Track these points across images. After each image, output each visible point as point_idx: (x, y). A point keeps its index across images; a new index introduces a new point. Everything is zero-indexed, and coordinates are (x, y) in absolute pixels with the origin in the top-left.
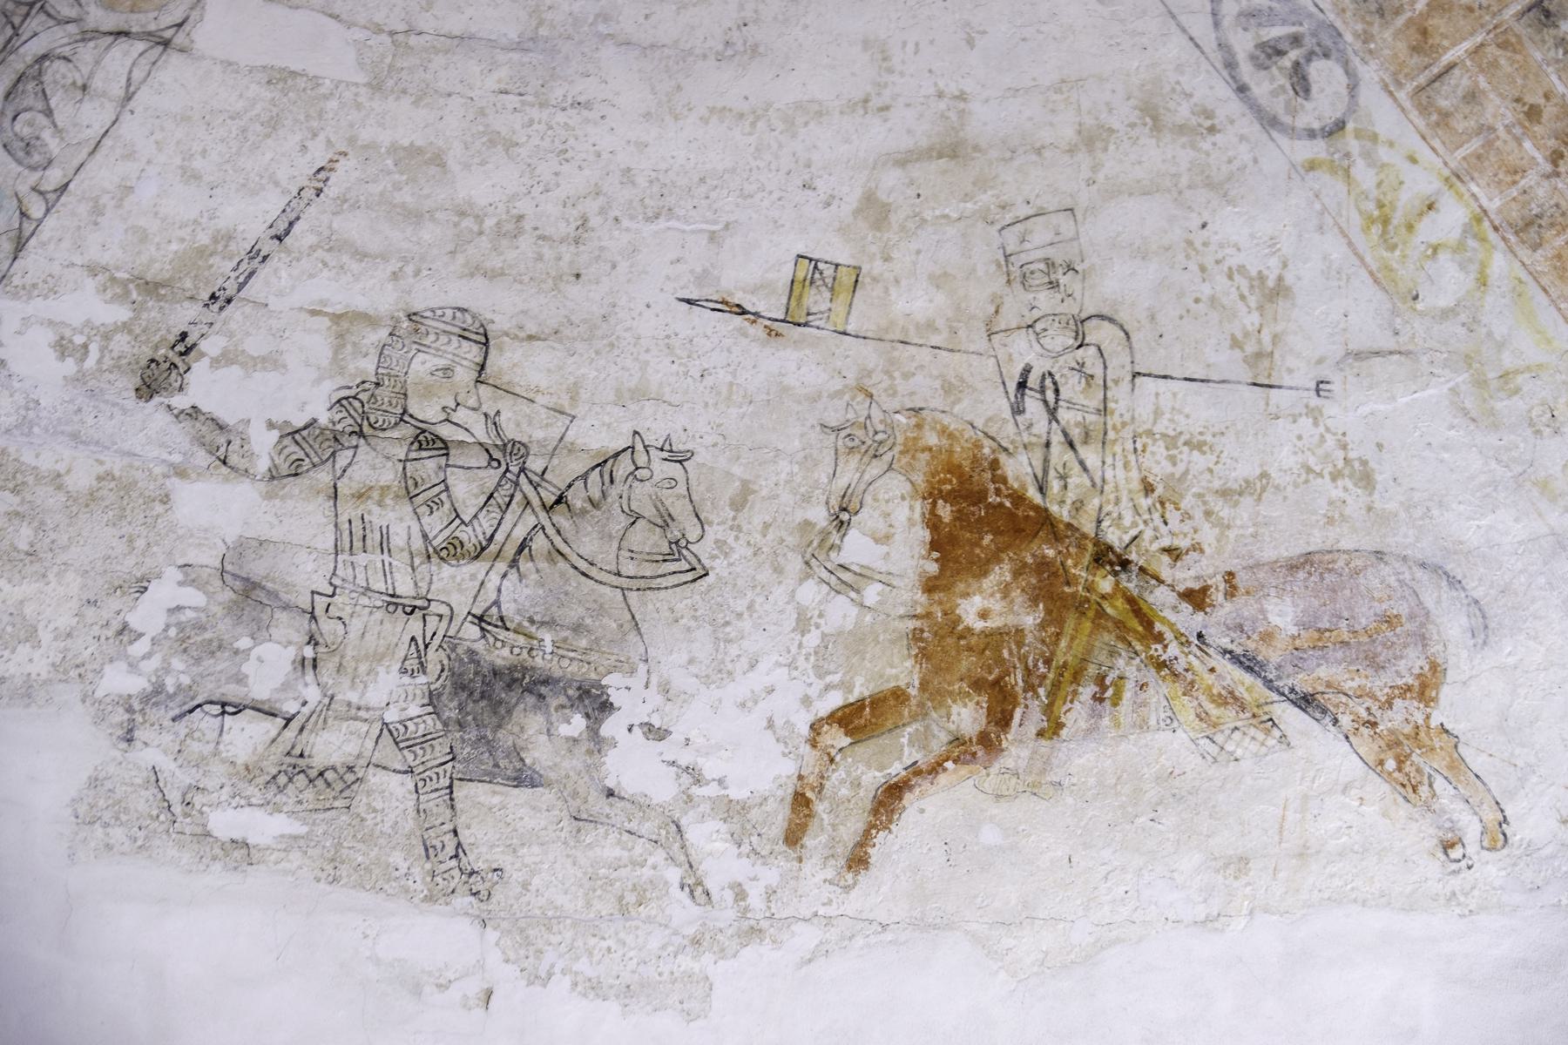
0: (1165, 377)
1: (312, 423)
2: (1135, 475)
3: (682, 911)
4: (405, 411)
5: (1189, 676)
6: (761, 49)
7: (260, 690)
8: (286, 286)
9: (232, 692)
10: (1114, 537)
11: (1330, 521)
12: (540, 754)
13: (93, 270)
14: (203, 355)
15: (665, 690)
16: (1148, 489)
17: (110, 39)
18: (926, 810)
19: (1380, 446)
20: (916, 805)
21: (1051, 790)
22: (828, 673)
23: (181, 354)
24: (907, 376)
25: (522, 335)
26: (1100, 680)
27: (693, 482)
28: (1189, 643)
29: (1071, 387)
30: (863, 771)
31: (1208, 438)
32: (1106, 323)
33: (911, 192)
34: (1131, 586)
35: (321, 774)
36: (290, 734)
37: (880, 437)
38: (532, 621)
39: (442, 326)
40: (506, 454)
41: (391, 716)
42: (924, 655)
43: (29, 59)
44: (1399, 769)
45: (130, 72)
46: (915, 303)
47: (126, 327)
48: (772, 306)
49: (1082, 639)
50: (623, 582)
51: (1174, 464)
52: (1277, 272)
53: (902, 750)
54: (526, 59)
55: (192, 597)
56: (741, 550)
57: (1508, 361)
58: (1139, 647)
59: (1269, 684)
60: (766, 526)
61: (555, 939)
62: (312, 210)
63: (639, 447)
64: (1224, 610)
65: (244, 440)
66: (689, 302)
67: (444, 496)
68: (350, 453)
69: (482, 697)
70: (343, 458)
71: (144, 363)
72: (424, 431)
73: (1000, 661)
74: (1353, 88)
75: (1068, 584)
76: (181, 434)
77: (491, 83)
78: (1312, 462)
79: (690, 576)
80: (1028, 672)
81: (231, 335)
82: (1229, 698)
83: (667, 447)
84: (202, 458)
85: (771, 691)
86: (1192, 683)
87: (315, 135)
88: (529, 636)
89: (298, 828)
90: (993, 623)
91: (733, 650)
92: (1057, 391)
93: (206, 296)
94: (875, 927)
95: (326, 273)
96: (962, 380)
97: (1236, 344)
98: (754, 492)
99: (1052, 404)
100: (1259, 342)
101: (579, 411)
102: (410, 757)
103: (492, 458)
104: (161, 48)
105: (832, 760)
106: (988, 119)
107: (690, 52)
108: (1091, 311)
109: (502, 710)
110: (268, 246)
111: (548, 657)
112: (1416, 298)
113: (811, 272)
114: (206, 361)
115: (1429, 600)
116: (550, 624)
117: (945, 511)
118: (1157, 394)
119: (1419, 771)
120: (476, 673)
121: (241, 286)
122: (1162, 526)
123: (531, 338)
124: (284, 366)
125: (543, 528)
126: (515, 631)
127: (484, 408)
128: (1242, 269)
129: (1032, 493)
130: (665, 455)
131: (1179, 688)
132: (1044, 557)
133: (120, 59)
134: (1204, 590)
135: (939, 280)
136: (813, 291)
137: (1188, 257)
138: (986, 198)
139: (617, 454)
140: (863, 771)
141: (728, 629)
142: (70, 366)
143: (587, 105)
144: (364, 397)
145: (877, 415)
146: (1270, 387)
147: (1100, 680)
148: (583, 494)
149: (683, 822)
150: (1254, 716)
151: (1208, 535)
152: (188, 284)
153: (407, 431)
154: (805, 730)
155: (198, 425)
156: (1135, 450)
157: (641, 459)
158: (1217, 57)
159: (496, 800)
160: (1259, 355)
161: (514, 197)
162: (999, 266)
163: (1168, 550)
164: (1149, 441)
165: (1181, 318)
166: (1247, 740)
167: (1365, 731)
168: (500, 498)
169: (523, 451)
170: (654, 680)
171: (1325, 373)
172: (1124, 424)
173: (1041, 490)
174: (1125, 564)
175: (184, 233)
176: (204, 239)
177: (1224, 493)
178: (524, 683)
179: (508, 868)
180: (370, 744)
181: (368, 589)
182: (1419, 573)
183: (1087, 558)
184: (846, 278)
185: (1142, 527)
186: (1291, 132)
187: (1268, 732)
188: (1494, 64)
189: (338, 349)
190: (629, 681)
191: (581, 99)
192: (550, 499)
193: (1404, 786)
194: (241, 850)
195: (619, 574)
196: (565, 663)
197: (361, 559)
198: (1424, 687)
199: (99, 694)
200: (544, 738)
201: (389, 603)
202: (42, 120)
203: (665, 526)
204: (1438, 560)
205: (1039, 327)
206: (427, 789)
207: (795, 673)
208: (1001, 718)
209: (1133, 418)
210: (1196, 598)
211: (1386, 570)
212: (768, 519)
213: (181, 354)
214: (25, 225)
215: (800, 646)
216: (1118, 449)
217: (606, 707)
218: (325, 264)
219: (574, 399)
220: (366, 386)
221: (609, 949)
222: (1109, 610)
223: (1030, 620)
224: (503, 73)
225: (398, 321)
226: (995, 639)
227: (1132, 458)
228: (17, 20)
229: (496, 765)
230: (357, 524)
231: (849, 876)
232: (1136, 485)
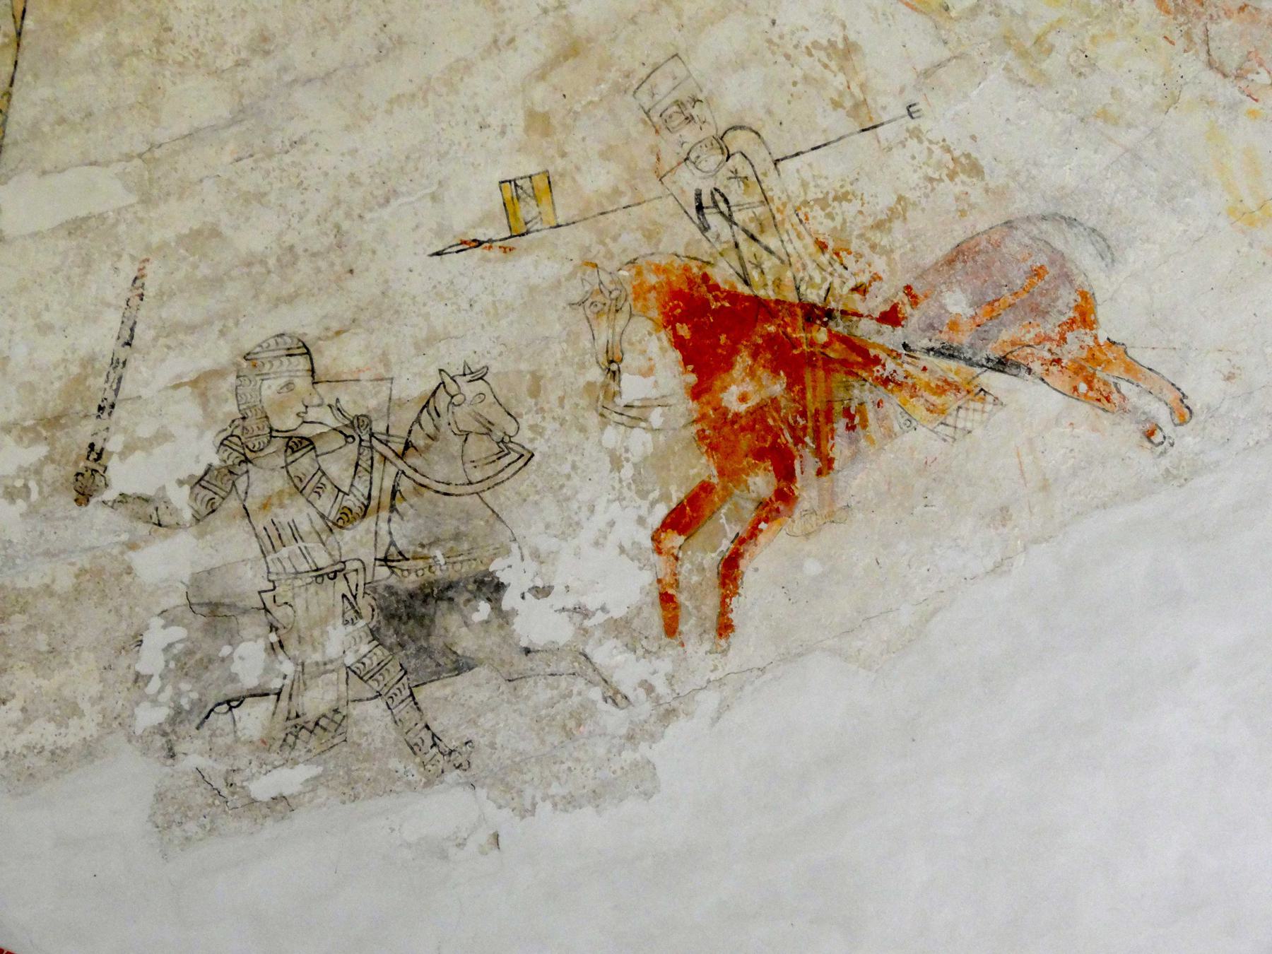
0: (797, 154)
1: (209, 469)
2: (809, 241)
3: (613, 719)
4: (271, 429)
5: (910, 381)
6: (405, 39)
7: (250, 681)
8: (149, 376)
9: (230, 691)
11: (963, 213)
12: (466, 643)
14: (111, 453)
15: (536, 555)
16: (823, 247)
18: (759, 568)
19: (973, 138)
20: (750, 568)
21: (843, 514)
22: (648, 493)
23: (96, 460)
24: (615, 239)
25: (330, 334)
26: (847, 413)
27: (496, 390)
28: (899, 355)
29: (735, 193)
30: (700, 558)
31: (848, 188)
33: (559, 96)
34: (840, 329)
35: (317, 724)
36: (284, 703)
37: (613, 296)
38: (422, 546)
39: (271, 354)
40: (356, 428)
41: (350, 659)
42: (713, 448)
44: (1091, 388)
46: (597, 179)
47: (49, 459)
48: (497, 230)
49: (822, 386)
51: (833, 219)
52: (841, 35)
53: (724, 527)
54: (244, 129)
55: (178, 633)
56: (550, 426)
57: (1036, 28)
58: (865, 375)
59: (969, 361)
60: (561, 400)
61: (528, 777)
62: (143, 312)
63: (447, 380)
64: (914, 317)
65: (167, 503)
66: (438, 254)
67: (324, 480)
68: (245, 478)
69: (409, 618)
70: (241, 484)
71: (72, 479)
72: (290, 438)
73: (768, 429)
75: (795, 348)
76: (118, 519)
77: (227, 158)
78: (930, 172)
79: (521, 462)
80: (792, 429)
81: (125, 430)
83: (467, 371)
84: (143, 529)
85: (612, 524)
86: (914, 386)
87: (119, 256)
88: (425, 558)
89: (315, 770)
90: (751, 403)
91: (574, 505)
92: (726, 201)
93: (95, 410)
94: (756, 672)
95: (172, 354)
96: (654, 223)
97: (836, 105)
98: (542, 377)
99: (727, 213)
100: (852, 95)
101: (395, 371)
102: (375, 684)
103: (347, 437)
105: (677, 559)
107: (356, 66)
108: (723, 126)
109: (427, 622)
110: (123, 353)
111: (444, 568)
112: (947, 9)
113: (514, 191)
114: (115, 458)
115: (1058, 244)
116: (436, 542)
117: (684, 331)
118: (798, 171)
119: (1106, 383)
120: (398, 602)
121: (117, 391)
122: (844, 272)
123: (338, 333)
124: (173, 436)
126: (414, 558)
127: (327, 402)
128: (816, 44)
129: (742, 289)
130: (469, 377)
131: (905, 393)
132: (769, 334)
134: (894, 308)
136: (522, 204)
137: (773, 53)
138: (613, 75)
139: (434, 393)
141: (565, 490)
142: (21, 505)
144: (238, 432)
145: (605, 278)
146: (875, 127)
147: (847, 413)
148: (422, 434)
149: (588, 651)
150: (968, 392)
151: (880, 265)
153: (279, 443)
154: (649, 544)
155: (129, 506)
156: (801, 221)
157: (452, 388)
159: (448, 691)
160: (856, 106)
161: (280, 234)
162: (645, 123)
163: (856, 289)
164: (808, 209)
165: (789, 102)
166: (970, 413)
167: (1055, 369)
168: (365, 464)
169: (366, 421)
170: (526, 552)
171: (910, 97)
173: (746, 282)
174: (829, 314)
175: (60, 371)
176: (75, 369)
177: (879, 226)
178: (435, 594)
179: (475, 738)
180: (343, 687)
181: (297, 573)
182: (1045, 226)
183: (800, 322)
185: (830, 279)
187: (983, 400)
189: (205, 405)
190: (508, 561)
191: (295, 139)
193: (1099, 400)
194: (282, 804)
195: (470, 483)
196: (458, 566)
197: (284, 552)
198: (1083, 315)
199: (139, 732)
200: (464, 629)
201: (316, 577)
203: (489, 433)
204: (1052, 209)
205: (693, 156)
206: (396, 702)
207: (624, 503)
208: (785, 472)
209: (788, 196)
210: (891, 317)
211: (1018, 234)
212: (561, 393)
215: (621, 481)
216: (788, 226)
217: (499, 587)
218: (169, 347)
219: (387, 365)
220: (236, 423)
221: (569, 769)
222: (832, 355)
223: (777, 387)
224: (231, 146)
226: (758, 414)
227: (801, 228)
229: (438, 665)
231: (723, 642)
232: (813, 248)
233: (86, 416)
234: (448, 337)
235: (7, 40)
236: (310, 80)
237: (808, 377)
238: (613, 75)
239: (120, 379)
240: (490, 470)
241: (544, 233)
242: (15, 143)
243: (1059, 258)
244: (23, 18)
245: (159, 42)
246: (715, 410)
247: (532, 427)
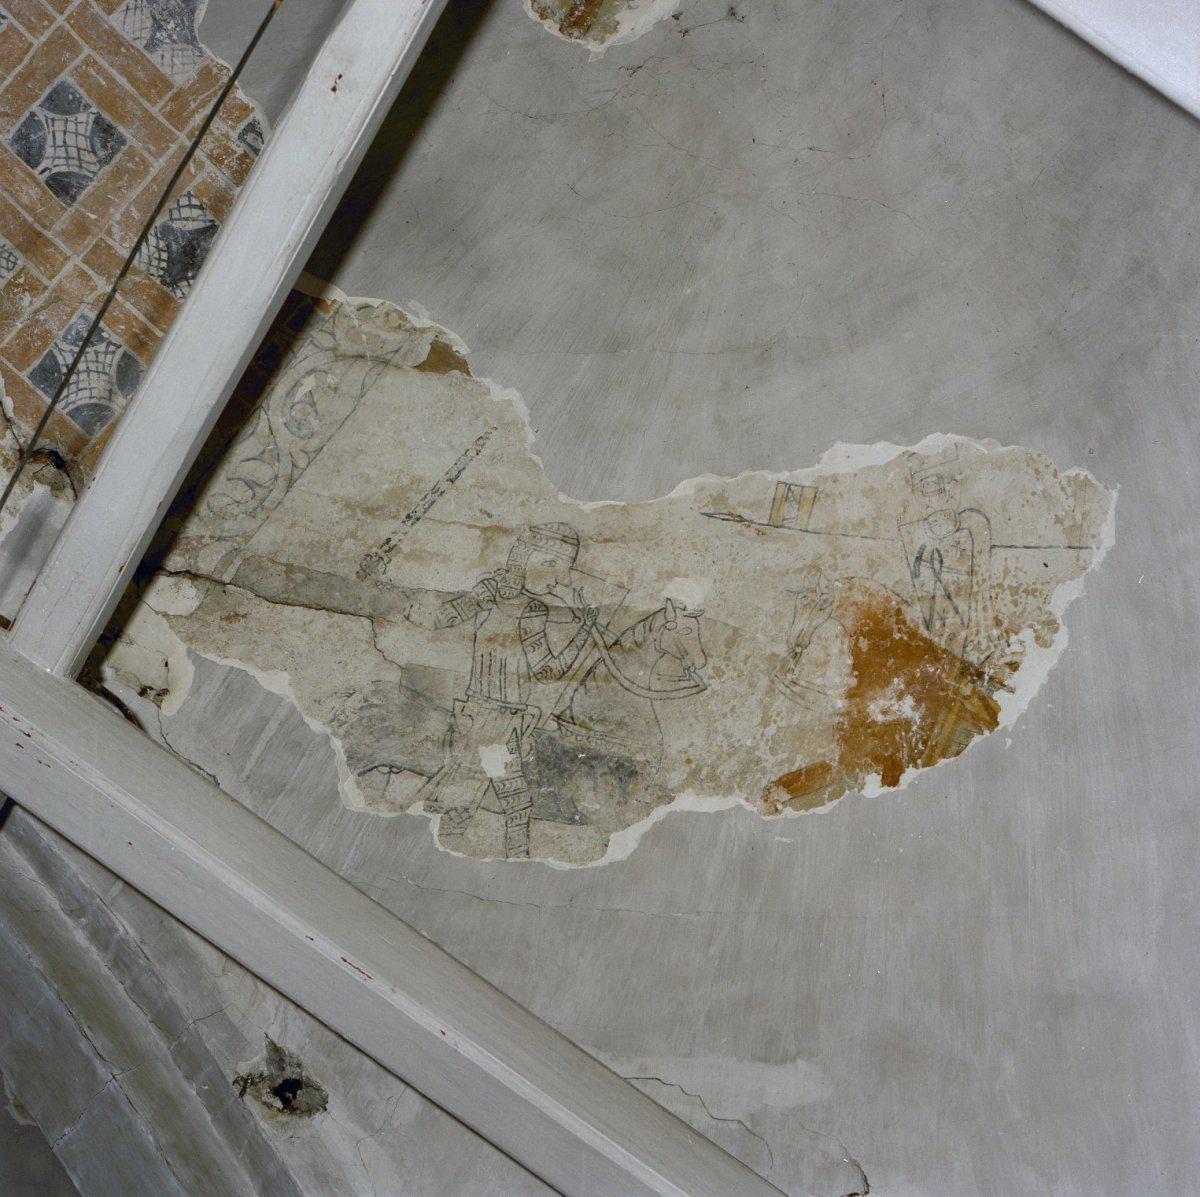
0: (1011, 547)
2: (990, 614)
4: (523, 587)
10: (974, 657)
16: (998, 623)
23: (386, 552)
24: (844, 557)
25: (600, 539)
31: (1039, 586)
32: (974, 514)
36: (430, 787)
37: (824, 597)
38: (591, 719)
40: (585, 617)
42: (845, 740)
45: (364, 380)
48: (761, 517)
50: (654, 695)
51: (1016, 606)
60: (747, 658)
63: (670, 608)
66: (710, 516)
67: (543, 641)
69: (555, 767)
72: (534, 600)
79: (694, 690)
80: (911, 749)
87: (478, 417)
88: (589, 729)
90: (890, 718)
93: (403, 516)
97: (1058, 520)
100: (1073, 519)
101: (635, 586)
103: (575, 616)
108: (965, 505)
116: (603, 721)
117: (864, 644)
118: (1006, 559)
120: (553, 752)
125: (604, 660)
127: (574, 585)
132: (927, 672)
133: (359, 371)
136: (787, 504)
137: (1028, 465)
139: (656, 613)
144: (498, 578)
145: (823, 583)
146: (1080, 548)
152: (393, 510)
153: (525, 600)
156: (991, 597)
157: (670, 615)
159: (556, 833)
162: (907, 481)
165: (1023, 506)
168: (578, 642)
172: (984, 580)
173: (928, 628)
175: (391, 478)
176: (405, 481)
180: (480, 794)
184: (809, 494)
185: (993, 649)
192: (610, 641)
195: (649, 689)
201: (502, 707)
202: (310, 409)
203: (682, 658)
205: (931, 519)
206: (513, 824)
209: (990, 577)
212: (748, 653)
213: (386, 552)
214: (295, 472)
215: (763, 735)
216: (979, 597)
222: (969, 707)
227: (988, 603)
229: (559, 811)
230: (486, 659)
232: (990, 622)
233: (395, 517)
237: (941, 717)
239: (433, 503)
241: (793, 532)
246: (859, 712)
247: (714, 668)
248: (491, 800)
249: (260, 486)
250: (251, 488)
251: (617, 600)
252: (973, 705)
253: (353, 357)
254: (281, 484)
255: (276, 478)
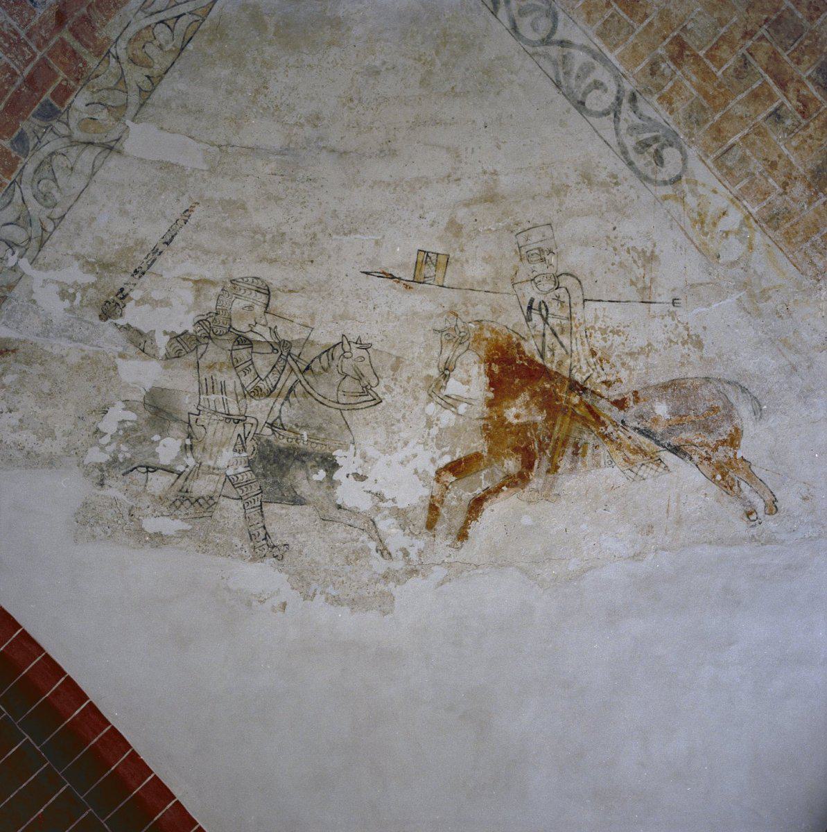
0: (599, 301)
1: (185, 332)
2: (587, 348)
3: (379, 564)
4: (231, 326)
5: (619, 441)
8: (174, 266)
9: (151, 461)
10: (578, 377)
11: (683, 364)
12: (304, 489)
13: (77, 257)
14: (132, 299)
15: (364, 457)
16: (594, 354)
17: (81, 147)
18: (494, 510)
19: (705, 328)
20: (489, 508)
21: (555, 498)
22: (443, 446)
23: (121, 299)
24: (474, 305)
25: (286, 290)
26: (576, 445)
27: (373, 359)
28: (618, 425)
29: (554, 308)
30: (460, 494)
31: (622, 328)
32: (569, 277)
34: (588, 400)
35: (197, 500)
36: (181, 481)
37: (462, 334)
39: (246, 286)
40: (281, 347)
41: (230, 472)
42: (490, 436)
43: (46, 154)
44: (723, 479)
45: (94, 162)
46: (476, 271)
47: (94, 285)
49: (566, 426)
51: (606, 342)
52: (651, 249)
53: (482, 481)
55: (131, 416)
56: (398, 390)
57: (764, 285)
58: (593, 429)
59: (657, 442)
60: (409, 378)
61: (317, 578)
63: (345, 342)
64: (633, 409)
65: (153, 340)
66: (367, 273)
67: (251, 367)
68: (205, 346)
70: (201, 349)
71: (103, 303)
72: (240, 336)
74: (684, 160)
75: (557, 400)
76: (120, 337)
77: (267, 170)
78: (672, 337)
79: (373, 403)
80: (540, 443)
81: (145, 290)
82: (639, 450)
83: (359, 342)
84: (132, 350)
85: (415, 456)
86: (620, 444)
89: (186, 526)
90: (520, 421)
91: (396, 437)
92: (547, 310)
93: (132, 271)
94: (473, 566)
96: (500, 306)
97: (632, 283)
99: (545, 316)
100: (644, 282)
102: (240, 492)
103: (274, 349)
104: (108, 151)
105: (447, 488)
106: (505, 183)
108: (561, 271)
109: (284, 468)
111: (306, 443)
112: (719, 257)
113: (425, 257)
114: (133, 302)
115: (733, 399)
116: (306, 427)
117: (496, 368)
118: (596, 309)
119: (733, 479)
120: (270, 451)
121: (149, 266)
122: (601, 371)
123: (290, 291)
124: (171, 305)
125: (300, 382)
126: (289, 431)
127: (269, 325)
128: (634, 248)
129: (538, 359)
130: (358, 346)
131: (614, 447)
132: (545, 388)
133: (88, 155)
134: (624, 400)
135: (487, 260)
136: (427, 267)
137: (608, 244)
138: (508, 220)
139: (335, 346)
140: (460, 494)
141: (393, 427)
142: (67, 303)
143: (315, 180)
145: (459, 323)
146: (650, 303)
147: (576, 445)
148: (319, 365)
149: (376, 520)
150: (651, 458)
151: (624, 374)
152: (124, 265)
153: (231, 336)
154: (433, 474)
155: (130, 333)
156: (586, 336)
157: (347, 348)
158: (618, 150)
159: (284, 511)
160: (644, 288)
162: (516, 252)
163: (605, 382)
164: (593, 331)
166: (649, 470)
167: (706, 462)
168: (279, 367)
169: (289, 345)
170: (358, 452)
171: (677, 295)
172: (580, 324)
173: (542, 356)
174: (585, 389)
175: (120, 240)
176: (131, 243)
177: (631, 354)
178: (296, 456)
179: (291, 543)
180: (220, 486)
181: (216, 411)
182: (727, 386)
183: (566, 388)
184: (442, 260)
185: (591, 372)
186: (655, 183)
187: (658, 465)
188: (754, 143)
189: (197, 297)
190: (346, 454)
193: (726, 487)
194: (159, 539)
195: (338, 403)
196: (314, 445)
197: (212, 397)
198: (733, 440)
199: (86, 463)
200: (305, 481)
201: (226, 418)
202: (52, 184)
204: (736, 379)
205: (536, 280)
206: (249, 507)
207: (427, 447)
209: (585, 321)
210: (620, 404)
211: (711, 386)
213: (121, 299)
214: (44, 235)
215: (429, 434)
218: (190, 256)
220: (211, 314)
221: (343, 581)
222: (578, 412)
224: (273, 165)
225: (226, 283)
226: (524, 428)
227: (585, 340)
228: (40, 135)
229: (283, 495)
230: (209, 381)
231: (459, 543)
232: (587, 352)
233: (126, 272)
234: (354, 319)
235: (174, 49)
236: (333, 151)
237: (559, 419)
238: (508, 220)
240: (353, 400)
241: (432, 286)
242: (153, 105)
243: (729, 406)
244: (188, 42)
245: (257, 91)
246: (499, 417)
247: (385, 386)
248: (228, 489)
249: (17, 245)
250: (11, 247)
251: (304, 336)
252: (581, 411)
253: (84, 143)
254: (34, 244)
255: (30, 239)
